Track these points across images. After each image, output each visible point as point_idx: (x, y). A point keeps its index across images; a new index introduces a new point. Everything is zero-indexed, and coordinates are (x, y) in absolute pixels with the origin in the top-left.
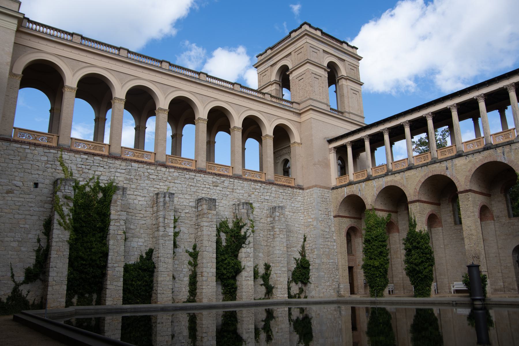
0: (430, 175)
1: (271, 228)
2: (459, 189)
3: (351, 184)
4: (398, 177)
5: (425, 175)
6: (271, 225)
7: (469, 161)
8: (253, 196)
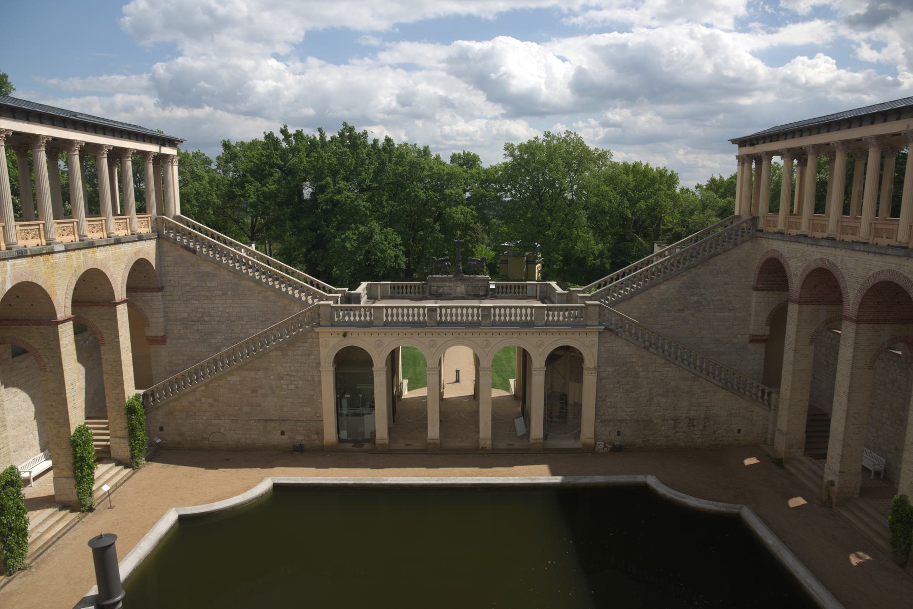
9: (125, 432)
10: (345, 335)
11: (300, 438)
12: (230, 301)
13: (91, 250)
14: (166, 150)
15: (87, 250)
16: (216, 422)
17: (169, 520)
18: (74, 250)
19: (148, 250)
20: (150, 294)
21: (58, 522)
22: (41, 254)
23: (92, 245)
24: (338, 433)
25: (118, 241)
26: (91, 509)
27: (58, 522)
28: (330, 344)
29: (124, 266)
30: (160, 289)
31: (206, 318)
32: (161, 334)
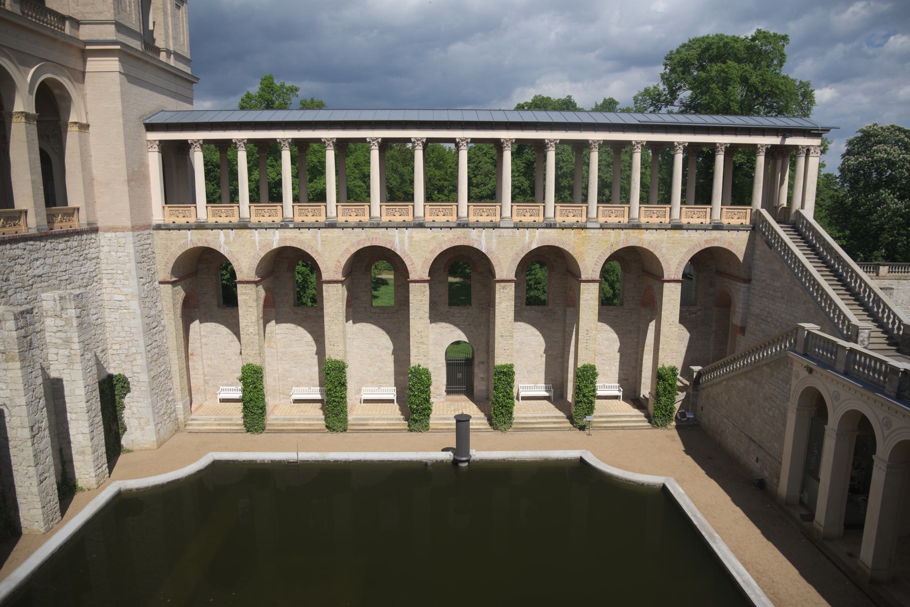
0: (367, 244)
1: (60, 341)
2: (412, 276)
3: (201, 226)
4: (307, 234)
5: (359, 242)
6: (63, 335)
7: (434, 238)
8: (12, 277)
9: (654, 393)
10: (810, 371)
11: (766, 474)
12: (784, 306)
13: (637, 231)
14: (790, 141)
15: (631, 231)
16: (725, 420)
17: (573, 454)
18: (613, 229)
19: (737, 243)
20: (739, 284)
21: (554, 423)
22: (573, 228)
23: (637, 227)
24: (802, 492)
25: (677, 227)
26: (582, 428)
27: (554, 423)
28: (801, 376)
29: (685, 250)
30: (748, 281)
31: (769, 319)
32: (739, 324)
